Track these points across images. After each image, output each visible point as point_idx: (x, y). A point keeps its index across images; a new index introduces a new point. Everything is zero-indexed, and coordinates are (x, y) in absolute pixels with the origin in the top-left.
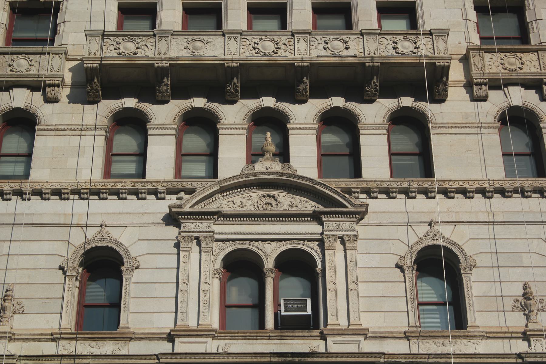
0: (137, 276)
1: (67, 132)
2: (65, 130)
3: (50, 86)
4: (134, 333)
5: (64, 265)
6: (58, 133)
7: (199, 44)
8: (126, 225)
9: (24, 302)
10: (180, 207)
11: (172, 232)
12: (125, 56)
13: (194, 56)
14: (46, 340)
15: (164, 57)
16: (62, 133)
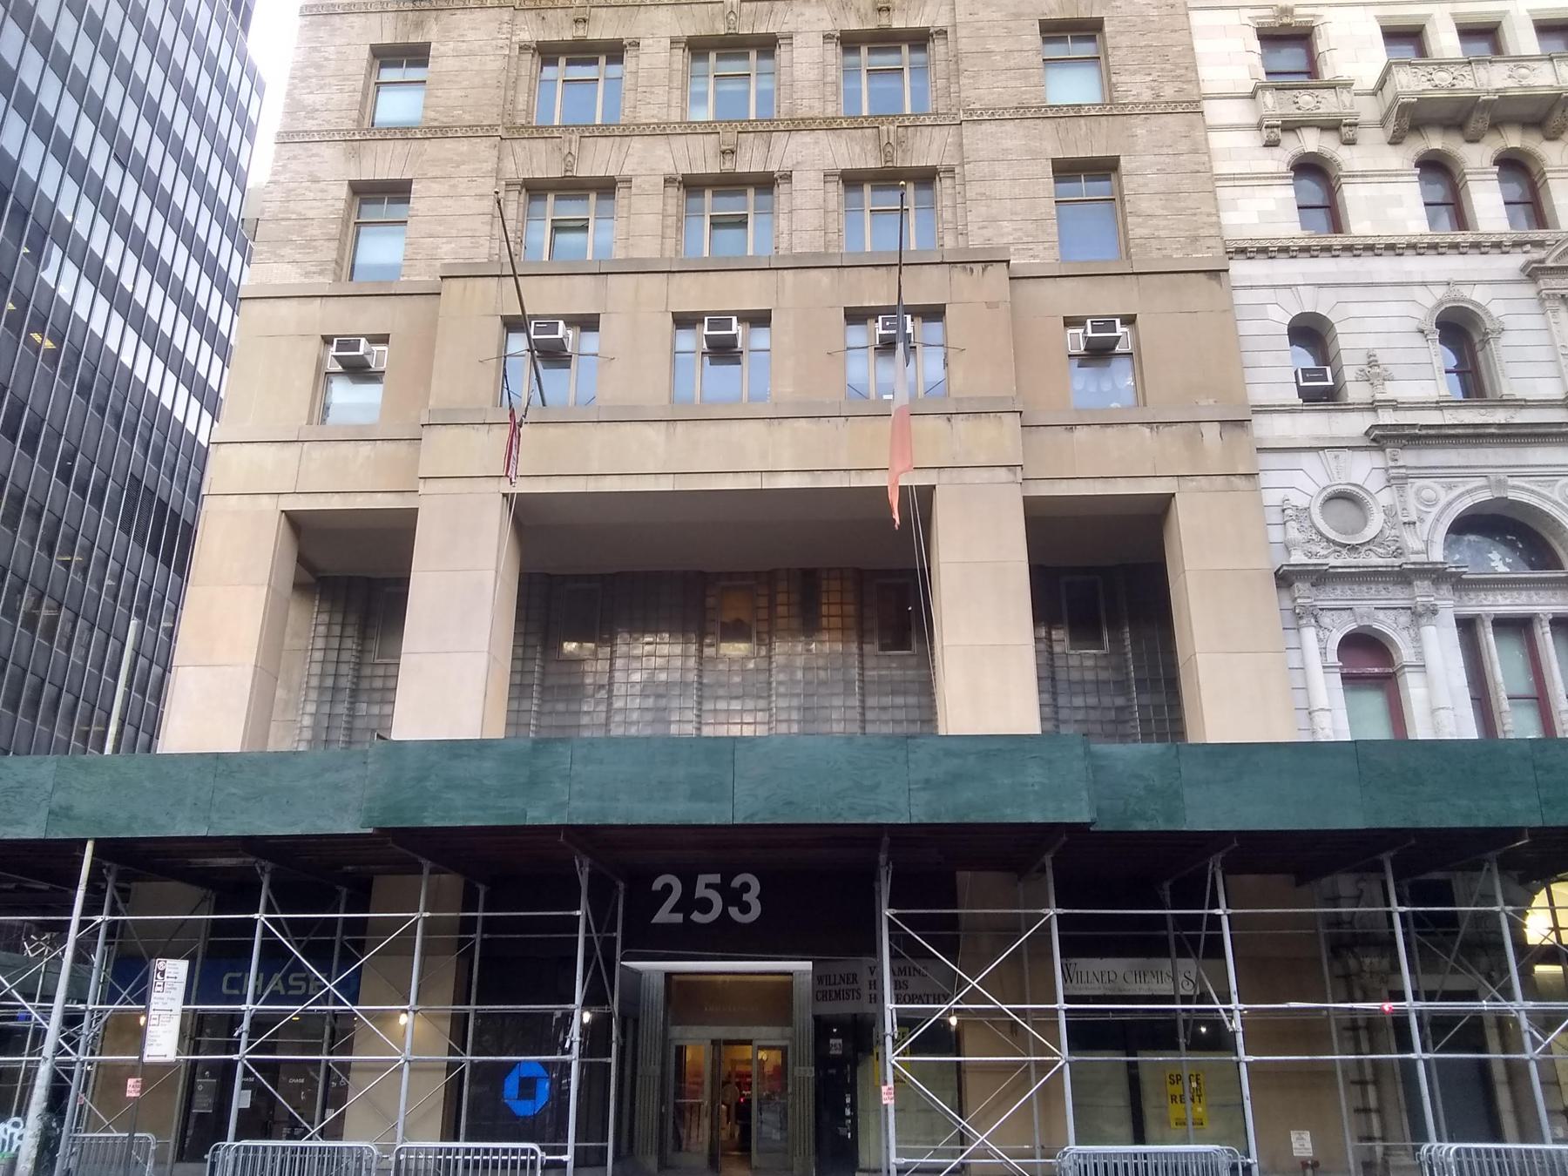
0: (1506, 339)
1: (1376, 179)
2: (1372, 176)
3: (1345, 125)
4: (1525, 401)
5: (1422, 327)
6: (1366, 180)
7: (1523, 71)
8: (1475, 283)
9: (1391, 368)
10: (1542, 261)
11: (1529, 290)
12: (1442, 88)
13: (1522, 87)
14: (1430, 408)
15: (1490, 88)
16: (1369, 180)
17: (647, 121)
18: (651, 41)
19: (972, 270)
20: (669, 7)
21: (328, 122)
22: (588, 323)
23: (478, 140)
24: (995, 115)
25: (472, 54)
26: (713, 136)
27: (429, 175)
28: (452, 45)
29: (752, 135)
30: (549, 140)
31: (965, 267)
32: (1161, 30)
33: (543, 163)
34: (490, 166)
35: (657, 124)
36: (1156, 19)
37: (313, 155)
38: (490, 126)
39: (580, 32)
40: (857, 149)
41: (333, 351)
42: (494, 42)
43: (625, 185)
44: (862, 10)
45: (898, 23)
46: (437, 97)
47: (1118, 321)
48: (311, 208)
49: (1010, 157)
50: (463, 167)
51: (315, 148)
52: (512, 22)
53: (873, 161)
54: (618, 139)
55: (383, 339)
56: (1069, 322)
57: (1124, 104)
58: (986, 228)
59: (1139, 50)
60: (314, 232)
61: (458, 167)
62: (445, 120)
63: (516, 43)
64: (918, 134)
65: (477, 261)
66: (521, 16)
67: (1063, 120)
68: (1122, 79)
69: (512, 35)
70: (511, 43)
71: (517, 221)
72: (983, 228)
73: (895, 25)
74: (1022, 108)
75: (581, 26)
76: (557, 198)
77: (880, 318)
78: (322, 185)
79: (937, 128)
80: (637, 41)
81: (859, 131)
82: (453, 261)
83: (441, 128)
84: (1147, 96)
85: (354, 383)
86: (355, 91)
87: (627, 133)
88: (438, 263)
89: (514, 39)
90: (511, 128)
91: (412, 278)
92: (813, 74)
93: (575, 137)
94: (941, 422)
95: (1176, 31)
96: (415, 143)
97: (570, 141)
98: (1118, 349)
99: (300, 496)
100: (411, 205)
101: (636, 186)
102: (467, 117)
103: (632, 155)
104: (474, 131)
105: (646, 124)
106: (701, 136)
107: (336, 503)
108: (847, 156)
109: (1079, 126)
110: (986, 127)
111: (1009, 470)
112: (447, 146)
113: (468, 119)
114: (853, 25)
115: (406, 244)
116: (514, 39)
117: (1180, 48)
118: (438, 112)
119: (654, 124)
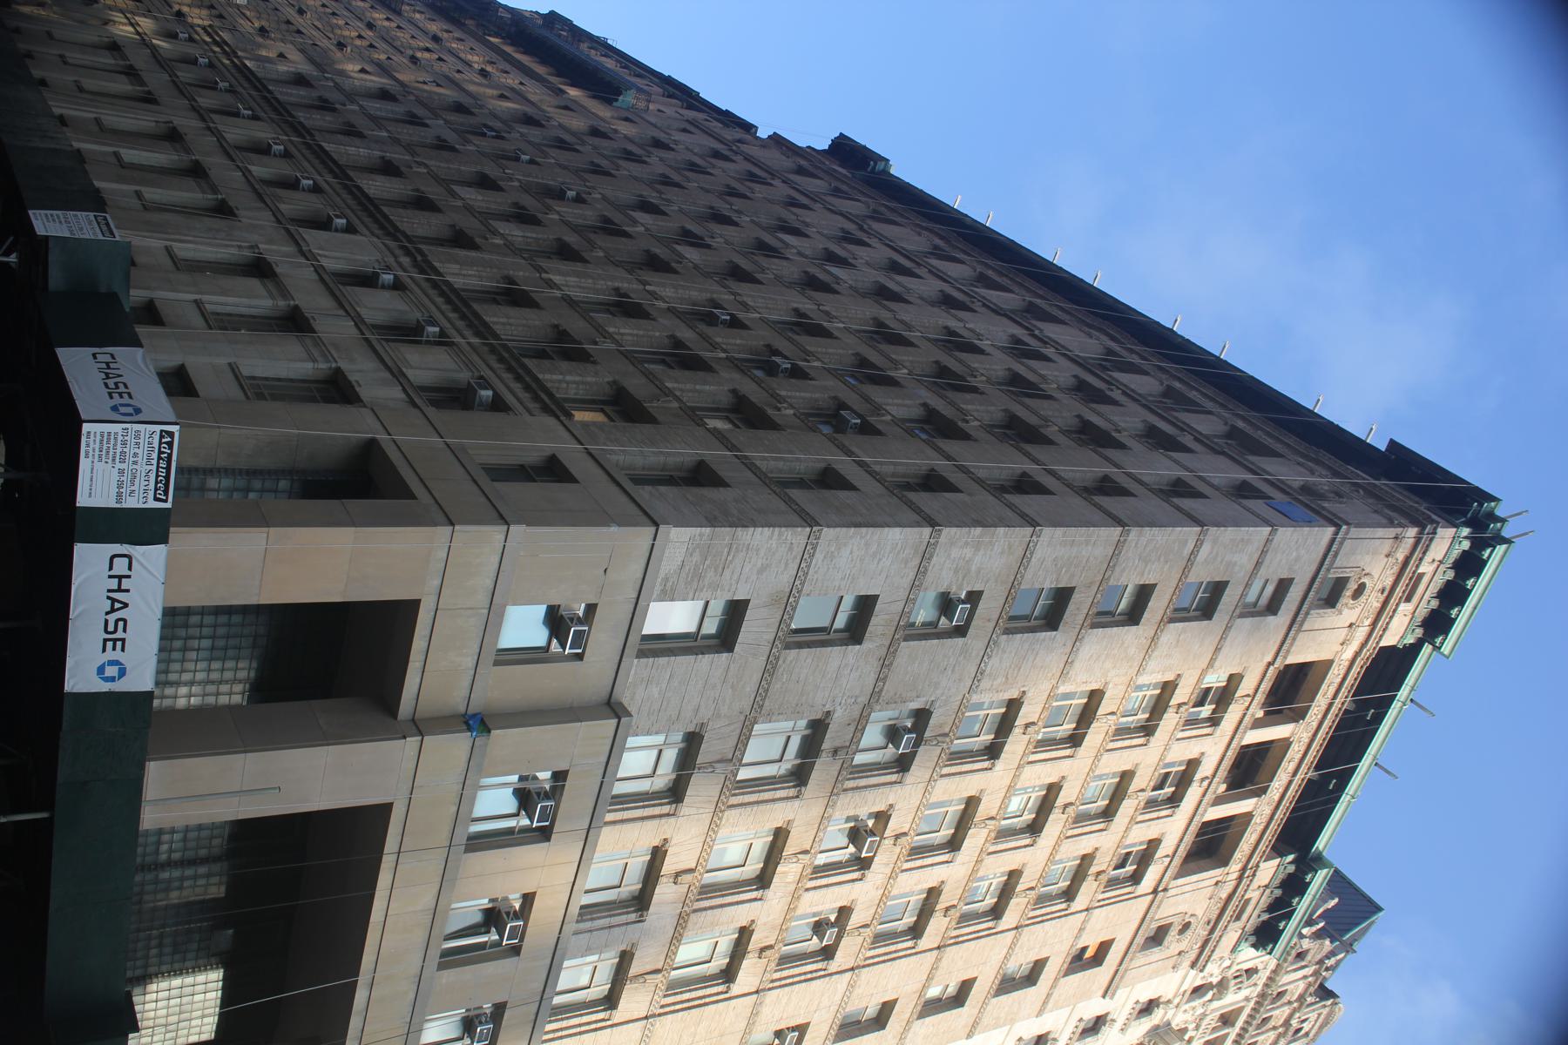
27: (732, 665)
37: (787, 564)
83: (774, 668)
85: (544, 623)
91: (634, 668)
99: (433, 613)
107: (418, 644)
118: (791, 662)
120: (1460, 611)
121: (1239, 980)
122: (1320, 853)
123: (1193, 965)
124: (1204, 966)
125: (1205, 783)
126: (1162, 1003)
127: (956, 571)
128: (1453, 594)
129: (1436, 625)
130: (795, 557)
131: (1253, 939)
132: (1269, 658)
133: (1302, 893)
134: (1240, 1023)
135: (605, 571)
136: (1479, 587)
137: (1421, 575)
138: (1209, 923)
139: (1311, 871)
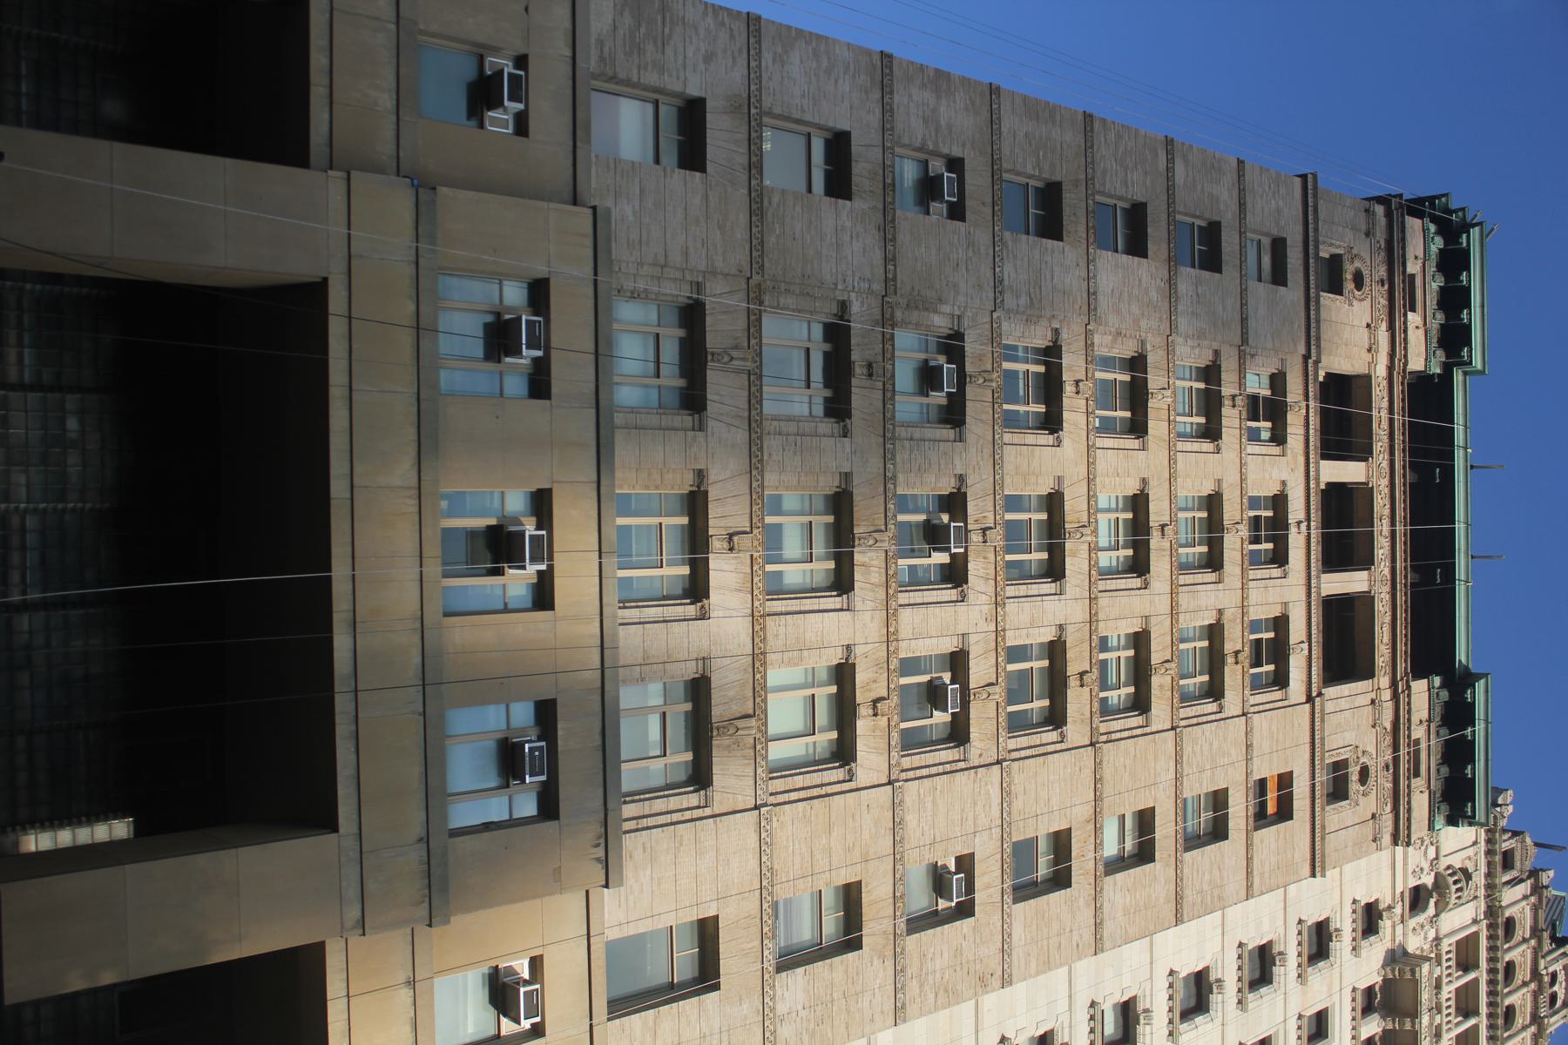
17: (765, 447)
18: (848, 450)
19: (598, 845)
20: (882, 470)
21: (770, 78)
22: (539, 385)
23: (748, 252)
24: (764, 845)
25: (839, 246)
26: (748, 525)
27: (710, 193)
28: (848, 224)
29: (749, 571)
30: (746, 334)
31: (599, 837)
32: (848, 1011)
33: (721, 329)
34: (719, 264)
35: (762, 460)
36: (860, 1005)
38: (763, 266)
39: (859, 370)
40: (731, 693)
41: (509, 68)
42: (850, 273)
43: (697, 423)
44: (874, 685)
45: (863, 725)
46: (794, 206)
47: (538, 1019)
48: (675, 52)
49: (720, 868)
50: (718, 232)
51: (742, 61)
52: (870, 291)
53: (718, 713)
54: (746, 414)
55: (522, 125)
56: (536, 964)
57: (774, 986)
58: (644, 851)
59: (829, 992)
60: (648, 54)
61: (719, 227)
62: (770, 214)
63: (849, 297)
64: (747, 761)
65: (613, 245)
66: (875, 303)
67: (758, 921)
68: (800, 978)
69: (857, 293)
70: (849, 292)
71: (656, 294)
72: (644, 848)
73: (859, 723)
74: (772, 874)
75: (865, 371)
76: (681, 339)
77: (543, 744)
78: (701, 66)
79: (753, 782)
80: (849, 435)
81: (751, 694)
82: (613, 221)
84: (781, 1008)
86: (803, 111)
87: (753, 425)
88: (609, 203)
89: (853, 295)
90: (760, 289)
92: (810, 636)
93: (749, 365)
94: (417, 830)
95: (847, 1028)
96: (745, 178)
97: (744, 359)
98: (504, 1020)
99: (327, 15)
100: (677, 170)
101: (695, 436)
102: (773, 239)
103: (729, 431)
104: (757, 245)
105: (762, 447)
106: (748, 511)
107: (318, 60)
108: (725, 681)
109: (752, 941)
110: (754, 838)
111: (358, 922)
112: (741, 216)
113: (771, 240)
114: (861, 677)
115: (633, 162)
116: (853, 295)
117: (830, 1035)
118: (778, 206)
119: (762, 455)
120: (1470, 314)
121: (1459, 886)
122: (1467, 668)
123: (1395, 842)
124: (1409, 836)
125: (1303, 526)
126: (1384, 910)
127: (925, 121)
128: (1454, 300)
129: (1453, 338)
130: (740, 51)
131: (1445, 808)
132: (1302, 350)
133: (1467, 341)
134: (1483, 955)
135: (526, 9)
136: (1474, 280)
137: (1412, 277)
138: (1387, 767)
139: (1468, 688)
